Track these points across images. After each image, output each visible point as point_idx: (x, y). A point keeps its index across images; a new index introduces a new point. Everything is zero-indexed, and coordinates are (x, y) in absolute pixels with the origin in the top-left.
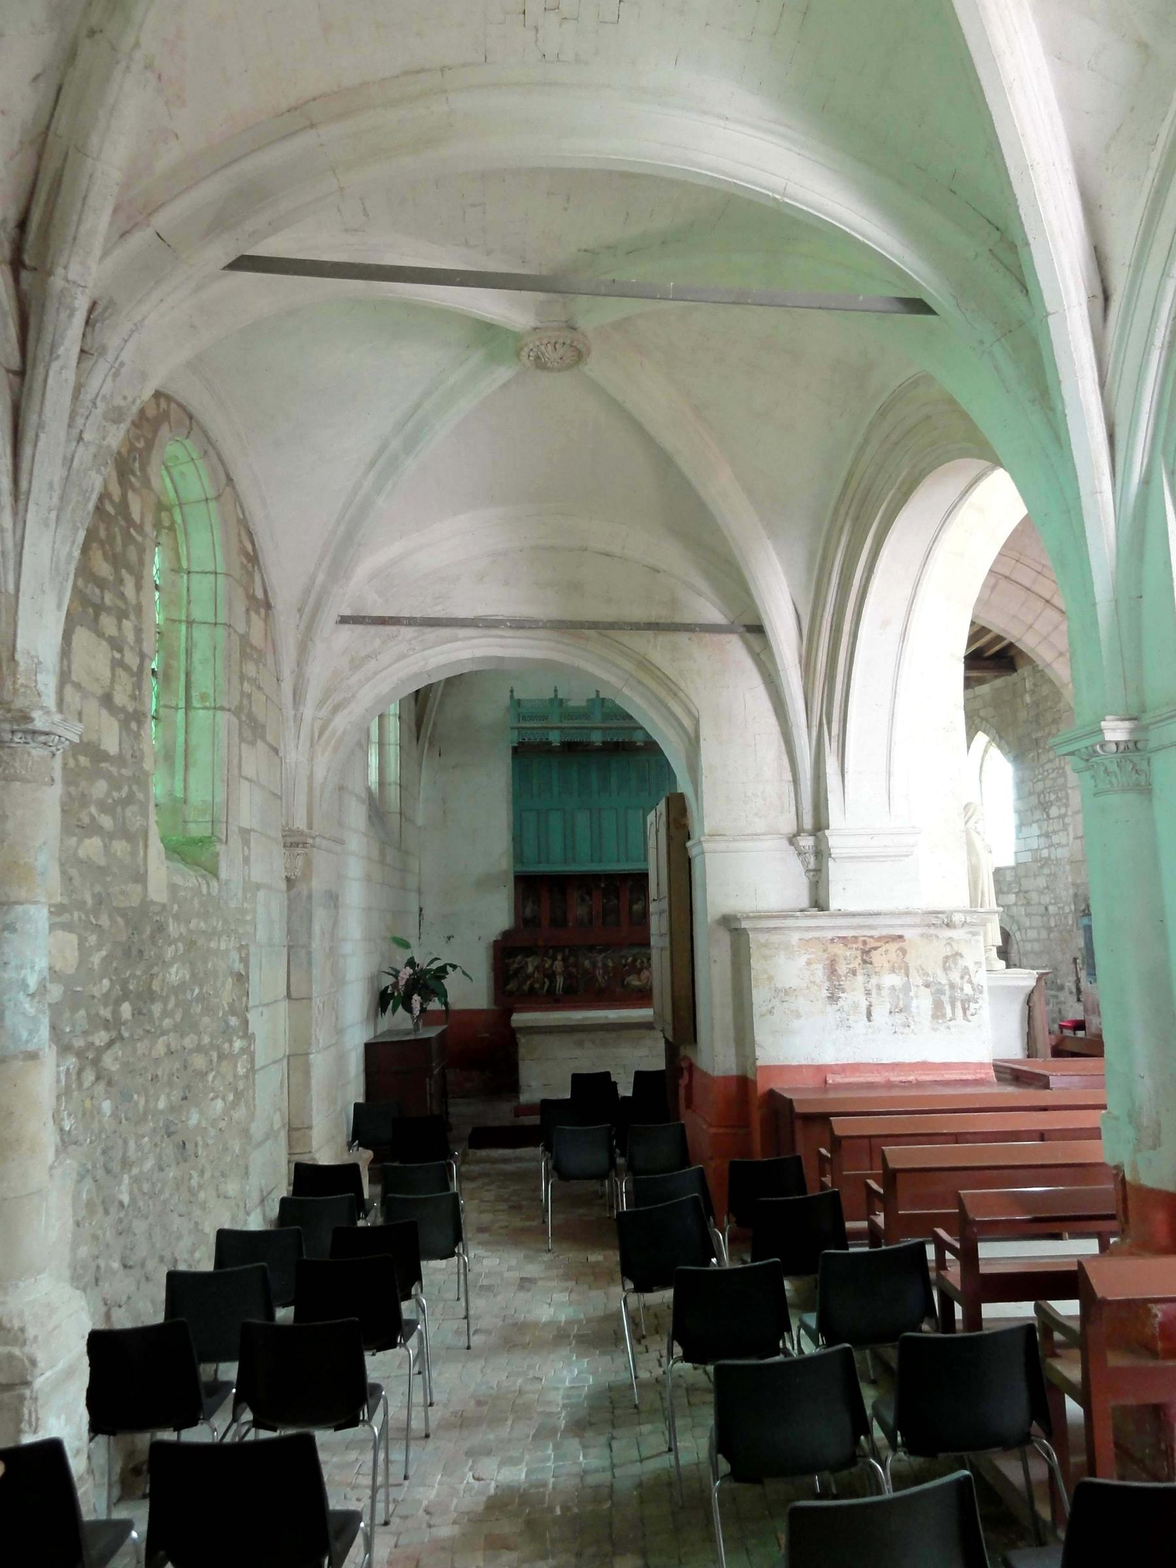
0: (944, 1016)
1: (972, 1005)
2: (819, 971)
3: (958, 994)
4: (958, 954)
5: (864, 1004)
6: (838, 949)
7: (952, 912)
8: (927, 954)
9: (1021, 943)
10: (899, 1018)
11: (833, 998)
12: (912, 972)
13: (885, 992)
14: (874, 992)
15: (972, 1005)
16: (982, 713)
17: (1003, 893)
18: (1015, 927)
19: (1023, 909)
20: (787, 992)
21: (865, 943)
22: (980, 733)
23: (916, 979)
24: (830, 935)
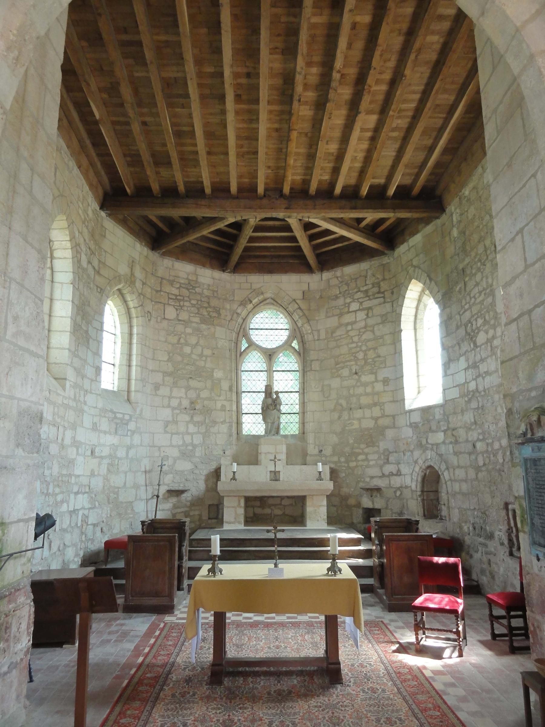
9: (449, 483)
16: (415, 263)
17: (433, 432)
18: (443, 467)
22: (413, 281)
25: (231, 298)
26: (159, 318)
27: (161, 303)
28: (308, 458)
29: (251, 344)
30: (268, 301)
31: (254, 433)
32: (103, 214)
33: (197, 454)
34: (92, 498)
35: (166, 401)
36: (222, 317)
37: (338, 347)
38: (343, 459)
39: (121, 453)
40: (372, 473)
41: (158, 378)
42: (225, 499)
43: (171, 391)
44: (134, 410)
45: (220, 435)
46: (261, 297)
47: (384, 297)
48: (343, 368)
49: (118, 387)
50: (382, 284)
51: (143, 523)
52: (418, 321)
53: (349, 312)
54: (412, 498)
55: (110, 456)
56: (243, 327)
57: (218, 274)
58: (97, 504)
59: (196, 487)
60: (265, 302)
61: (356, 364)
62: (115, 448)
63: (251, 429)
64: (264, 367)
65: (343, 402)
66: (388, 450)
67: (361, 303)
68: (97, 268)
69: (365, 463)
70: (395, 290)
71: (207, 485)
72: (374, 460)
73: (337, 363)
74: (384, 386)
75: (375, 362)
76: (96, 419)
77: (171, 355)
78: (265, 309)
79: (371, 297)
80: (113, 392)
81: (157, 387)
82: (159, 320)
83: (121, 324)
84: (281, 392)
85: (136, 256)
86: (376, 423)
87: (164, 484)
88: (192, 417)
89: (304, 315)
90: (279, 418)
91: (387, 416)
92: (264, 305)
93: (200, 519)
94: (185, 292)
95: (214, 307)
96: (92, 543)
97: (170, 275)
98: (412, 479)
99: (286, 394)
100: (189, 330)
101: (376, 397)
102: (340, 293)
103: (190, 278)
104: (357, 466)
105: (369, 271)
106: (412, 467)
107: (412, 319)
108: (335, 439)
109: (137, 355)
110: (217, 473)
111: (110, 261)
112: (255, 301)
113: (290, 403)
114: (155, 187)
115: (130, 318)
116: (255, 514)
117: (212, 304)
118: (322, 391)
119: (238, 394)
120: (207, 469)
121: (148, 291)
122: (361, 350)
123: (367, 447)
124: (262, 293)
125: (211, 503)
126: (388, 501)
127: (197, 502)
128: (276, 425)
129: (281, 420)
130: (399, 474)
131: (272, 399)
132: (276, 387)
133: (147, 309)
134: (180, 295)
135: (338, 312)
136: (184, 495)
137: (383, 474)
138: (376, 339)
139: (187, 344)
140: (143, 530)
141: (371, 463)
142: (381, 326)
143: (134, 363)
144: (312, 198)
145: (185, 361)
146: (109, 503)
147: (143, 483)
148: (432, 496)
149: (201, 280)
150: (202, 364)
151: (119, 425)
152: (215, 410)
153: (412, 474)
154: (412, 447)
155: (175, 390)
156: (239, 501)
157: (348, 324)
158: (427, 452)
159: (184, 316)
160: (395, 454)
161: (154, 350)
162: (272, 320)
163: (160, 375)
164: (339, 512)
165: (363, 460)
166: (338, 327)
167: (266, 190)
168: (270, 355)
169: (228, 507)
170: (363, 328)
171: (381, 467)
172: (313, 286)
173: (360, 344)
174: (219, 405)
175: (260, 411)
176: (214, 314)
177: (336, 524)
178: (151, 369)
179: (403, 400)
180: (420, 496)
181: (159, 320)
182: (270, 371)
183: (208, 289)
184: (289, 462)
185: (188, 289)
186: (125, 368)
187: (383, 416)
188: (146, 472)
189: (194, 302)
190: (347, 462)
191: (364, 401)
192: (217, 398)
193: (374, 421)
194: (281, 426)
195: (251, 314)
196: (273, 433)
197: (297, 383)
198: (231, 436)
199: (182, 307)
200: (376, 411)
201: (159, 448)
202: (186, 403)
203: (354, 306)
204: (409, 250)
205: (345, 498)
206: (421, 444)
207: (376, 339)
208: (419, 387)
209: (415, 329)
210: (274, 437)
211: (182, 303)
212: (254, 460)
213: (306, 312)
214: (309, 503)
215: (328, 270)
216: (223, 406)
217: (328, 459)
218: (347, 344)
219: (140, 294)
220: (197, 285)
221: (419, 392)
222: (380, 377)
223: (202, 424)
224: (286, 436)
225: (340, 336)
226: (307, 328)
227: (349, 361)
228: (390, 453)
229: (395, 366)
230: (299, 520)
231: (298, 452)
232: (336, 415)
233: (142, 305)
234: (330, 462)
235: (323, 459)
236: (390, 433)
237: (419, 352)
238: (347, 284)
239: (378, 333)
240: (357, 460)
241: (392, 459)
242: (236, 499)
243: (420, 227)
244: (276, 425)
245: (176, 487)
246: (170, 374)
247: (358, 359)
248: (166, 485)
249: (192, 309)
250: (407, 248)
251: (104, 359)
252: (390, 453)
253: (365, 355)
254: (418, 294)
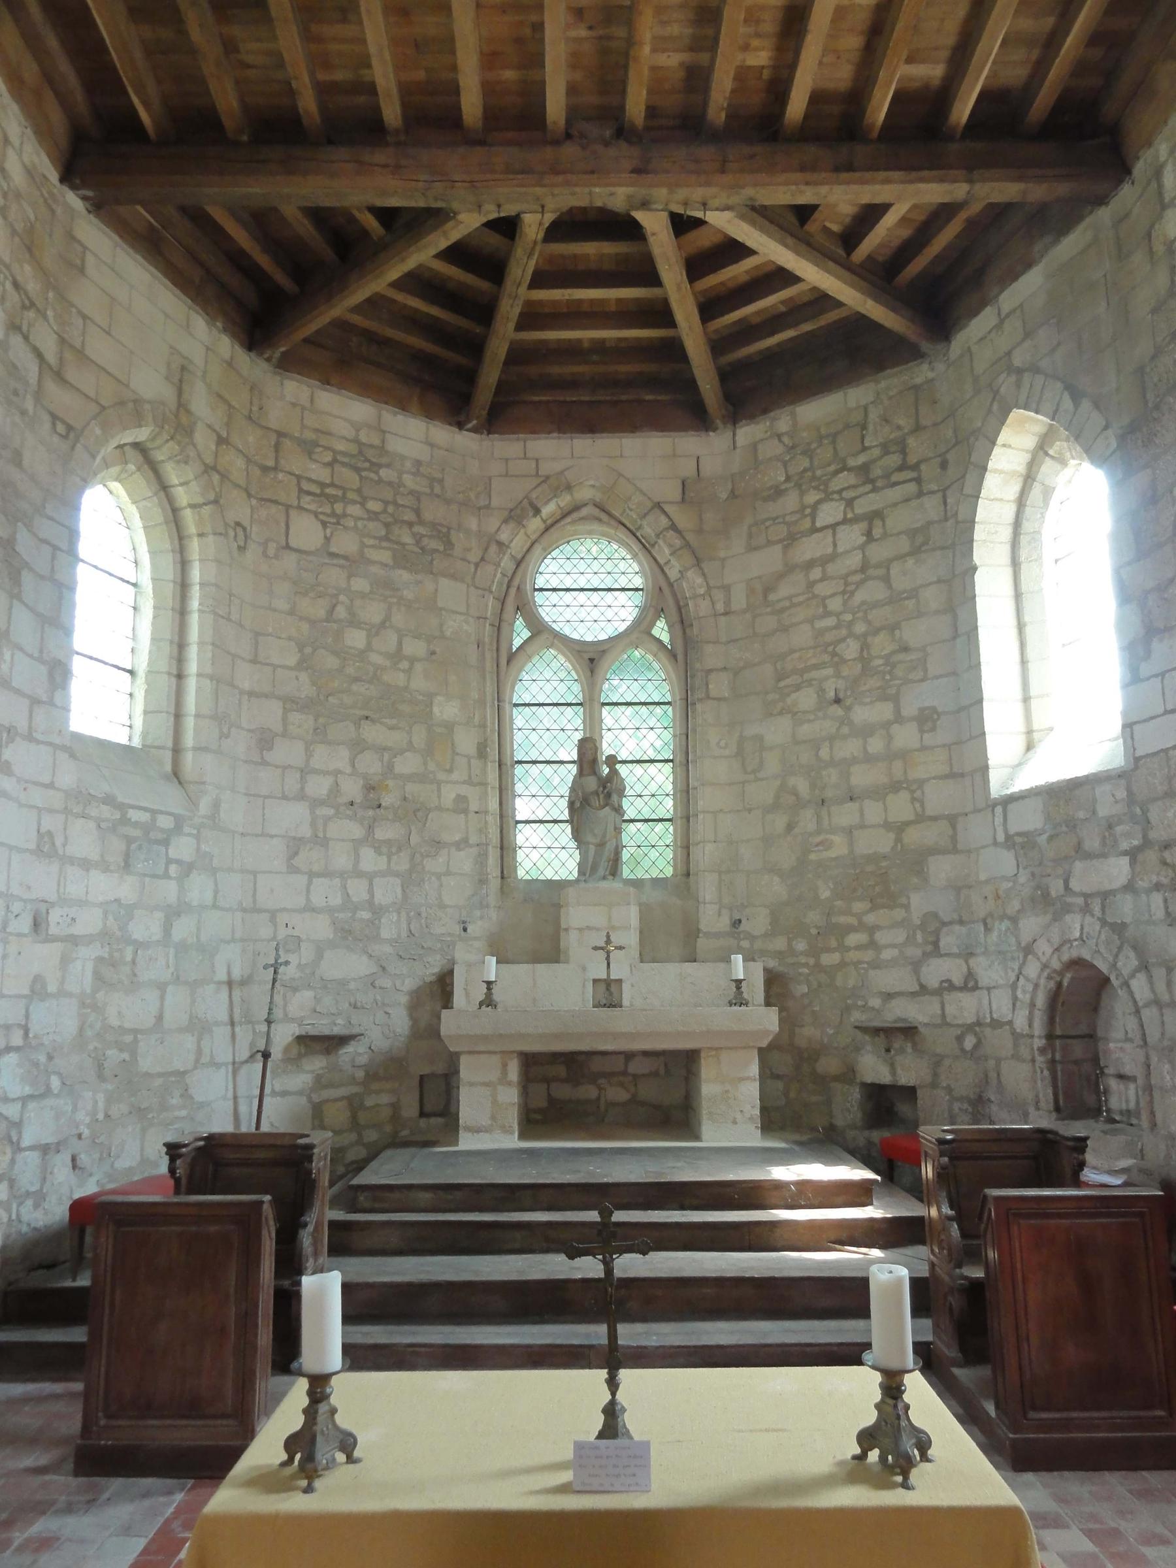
16: (1017, 361)
17: (1089, 856)
18: (1128, 961)
19: (1157, 899)
22: (1016, 414)
25: (482, 502)
26: (272, 548)
27: (276, 502)
28: (701, 942)
29: (539, 628)
30: (584, 512)
31: (549, 874)
32: (73, 199)
33: (385, 934)
34: (36, 1064)
35: (292, 782)
36: (457, 551)
37: (784, 629)
38: (801, 946)
39: (145, 927)
40: (889, 983)
41: (270, 714)
42: (464, 1061)
43: (309, 753)
44: (193, 802)
45: (454, 879)
46: (565, 500)
47: (918, 480)
48: (798, 688)
49: (144, 735)
50: (912, 442)
51: (173, 1150)
52: (1024, 540)
53: (815, 530)
54: (1016, 1057)
55: (104, 936)
56: (516, 583)
57: (442, 433)
58: (55, 1082)
59: (384, 1027)
60: (575, 515)
61: (838, 675)
62: (123, 911)
63: (541, 864)
64: (575, 692)
65: (802, 785)
66: (935, 915)
67: (850, 503)
68: (51, 357)
69: (869, 955)
70: (951, 457)
71: (414, 1021)
72: (894, 946)
73: (780, 676)
74: (922, 731)
75: (894, 666)
76: (48, 823)
77: (308, 650)
78: (575, 535)
79: (879, 484)
80: (127, 749)
81: (265, 740)
82: (271, 552)
83: (153, 553)
84: (624, 762)
85: (197, 354)
86: (898, 840)
87: (287, 1019)
88: (370, 829)
89: (687, 545)
90: (618, 831)
91: (935, 819)
92: (573, 522)
93: (395, 1117)
94: (349, 478)
95: (434, 525)
96: (36, 1206)
97: (303, 426)
98: (1015, 999)
99: (638, 769)
100: (360, 584)
101: (898, 765)
102: (788, 479)
103: (363, 438)
104: (843, 964)
105: (871, 408)
106: (1016, 966)
107: (1006, 533)
108: (777, 888)
109: (201, 644)
111: (99, 348)
112: (548, 510)
113: (649, 789)
114: (226, 99)
115: (181, 538)
116: (551, 1101)
117: (427, 516)
118: (740, 753)
119: (505, 767)
120: (412, 976)
121: (236, 465)
122: (851, 635)
123: (872, 910)
124: (569, 488)
125: (426, 1070)
126: (937, 1064)
127: (386, 1069)
128: (610, 846)
129: (625, 839)
130: (970, 984)
131: (599, 778)
133: (232, 516)
134: (332, 485)
135: (782, 531)
136: (350, 1049)
137: (922, 986)
138: (895, 599)
139: (354, 622)
140: (172, 1171)
141: (887, 954)
142: (910, 562)
143: (192, 667)
144: (718, 137)
145: (350, 670)
146: (101, 1077)
147: (225, 1017)
148: (1078, 1050)
149: (395, 445)
150: (400, 679)
151: (136, 843)
152: (439, 808)
153: (1014, 986)
154: (1015, 905)
155: (320, 751)
156: (505, 1065)
157: (810, 565)
158: (1068, 918)
159: (346, 543)
160: (957, 928)
161: (257, 634)
162: (596, 566)
163: (276, 707)
164: (792, 1095)
165: (858, 948)
166: (781, 576)
167: (573, 114)
168: (591, 660)
169: (471, 1084)
170: (856, 572)
171: (916, 966)
172: (710, 467)
173: (848, 617)
174: (449, 795)
175: (566, 815)
176: (434, 544)
177: (782, 1128)
178: (246, 685)
179: (985, 768)
180: (1042, 1051)
181: (271, 552)
182: (591, 704)
183: (417, 473)
184: (648, 953)
185: (357, 470)
186: (165, 683)
187: (921, 819)
188: (230, 984)
189: (374, 506)
190: (815, 952)
191: (862, 777)
192: (441, 776)
193: (892, 836)
194: (625, 855)
195: (537, 550)
196: (601, 872)
197: (667, 736)
198: (483, 881)
199: (339, 518)
200: (900, 807)
201: (273, 914)
202: (352, 789)
203: (830, 513)
204: (999, 326)
205: (806, 1057)
206: (1046, 895)
207: (895, 599)
208: (1029, 732)
209: (1015, 564)
210: (604, 884)
211: (339, 508)
212: (549, 950)
213: (690, 537)
214: (707, 1070)
215: (752, 417)
216: (461, 799)
217: (758, 945)
218: (811, 621)
219: (209, 469)
220: (384, 460)
221: (1029, 747)
222: (910, 708)
223: (400, 849)
224: (637, 884)
225: (790, 598)
226: (693, 583)
227: (816, 667)
228: (944, 924)
229: (954, 674)
230: (677, 1117)
231: (673, 926)
232: (780, 822)
233: (216, 502)
234: (763, 953)
235: (745, 944)
236: (941, 869)
237: (1028, 630)
238: (808, 453)
239: (900, 583)
240: (842, 948)
241: (948, 941)
242: (495, 1060)
243: (1038, 247)
244: (610, 846)
245: (323, 1027)
246: (305, 706)
247: (845, 661)
248: (293, 1020)
249: (371, 525)
250: (994, 321)
251: (79, 641)
252: (944, 924)
253: (865, 646)
254: (1024, 458)
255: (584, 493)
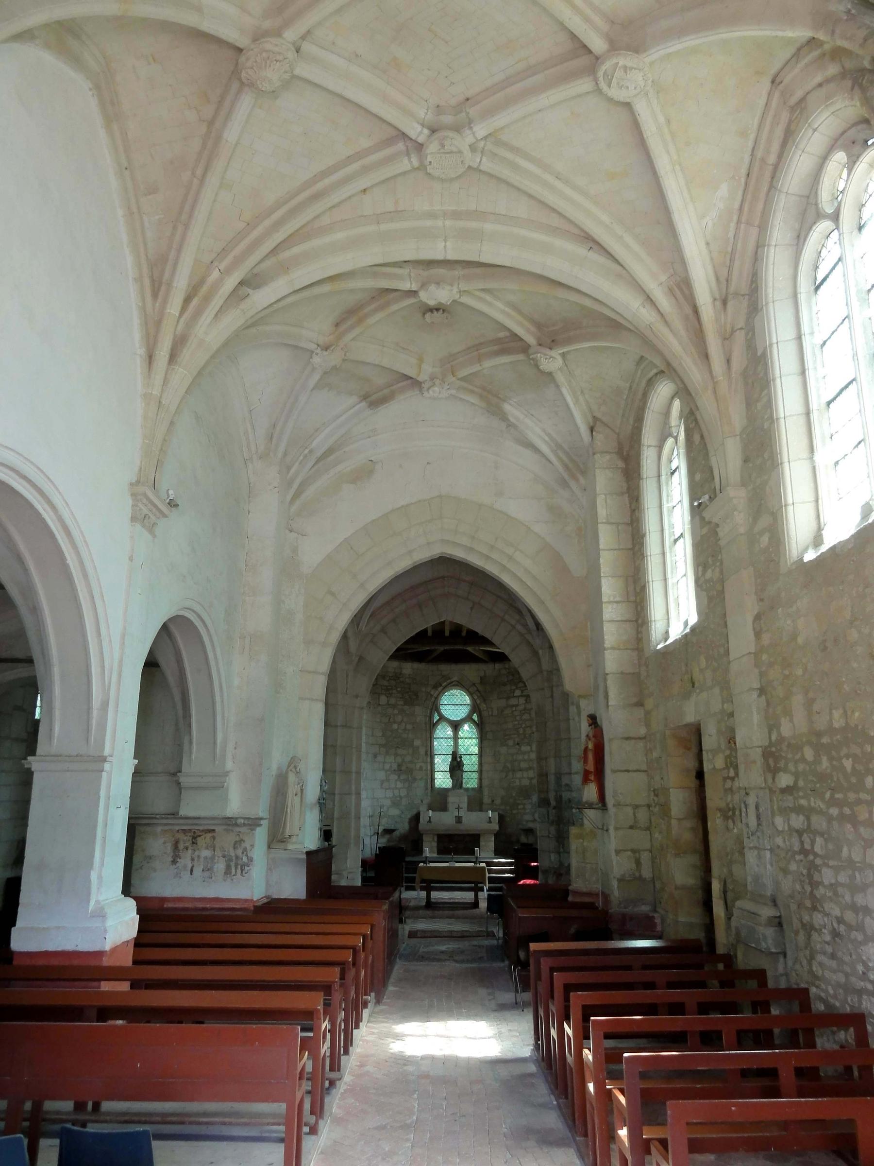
0: (230, 873)
1: (247, 868)
2: (169, 847)
3: (239, 862)
4: (242, 840)
5: (190, 866)
6: (181, 836)
7: (237, 818)
8: (226, 840)
10: (207, 874)
11: (174, 862)
12: (217, 849)
13: (202, 860)
14: (196, 859)
15: (247, 868)
20: (150, 858)
21: (194, 833)
23: (218, 853)
24: (177, 828)
28: (484, 807)
29: (442, 718)
31: (444, 786)
38: (508, 808)
45: (419, 789)
46: (449, 681)
57: (416, 665)
59: (403, 827)
65: (509, 765)
81: (375, 756)
90: (462, 776)
94: (393, 683)
100: (396, 712)
108: (502, 793)
110: (416, 818)
113: (470, 763)
120: (409, 815)
127: (404, 838)
132: (462, 750)
139: (395, 722)
149: (404, 671)
157: (513, 706)
159: (392, 701)
174: (418, 766)
182: (456, 738)
184: (470, 809)
191: (523, 765)
198: (427, 789)
202: (395, 766)
216: (421, 768)
224: (467, 789)
226: (483, 706)
231: (476, 802)
238: (513, 675)
253: (524, 731)
255: (455, 679)
